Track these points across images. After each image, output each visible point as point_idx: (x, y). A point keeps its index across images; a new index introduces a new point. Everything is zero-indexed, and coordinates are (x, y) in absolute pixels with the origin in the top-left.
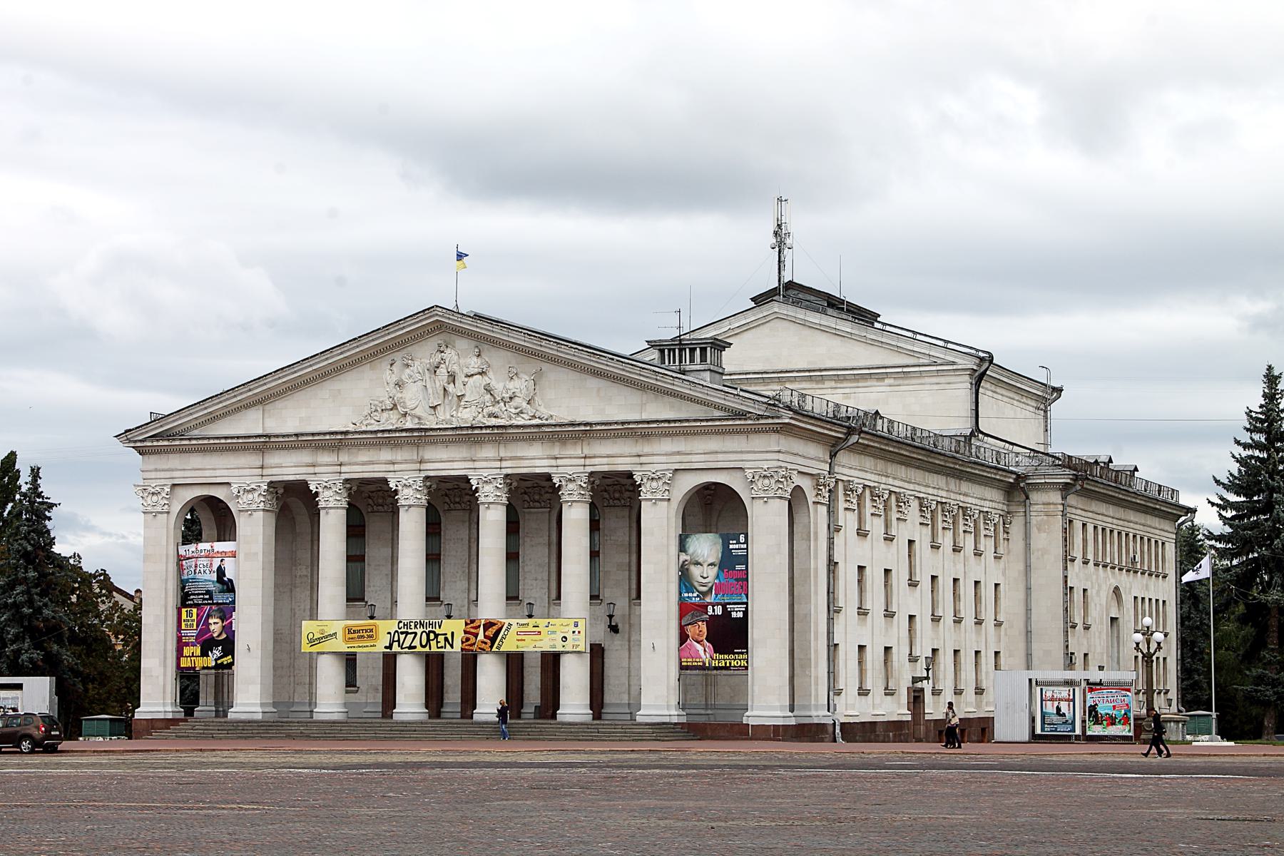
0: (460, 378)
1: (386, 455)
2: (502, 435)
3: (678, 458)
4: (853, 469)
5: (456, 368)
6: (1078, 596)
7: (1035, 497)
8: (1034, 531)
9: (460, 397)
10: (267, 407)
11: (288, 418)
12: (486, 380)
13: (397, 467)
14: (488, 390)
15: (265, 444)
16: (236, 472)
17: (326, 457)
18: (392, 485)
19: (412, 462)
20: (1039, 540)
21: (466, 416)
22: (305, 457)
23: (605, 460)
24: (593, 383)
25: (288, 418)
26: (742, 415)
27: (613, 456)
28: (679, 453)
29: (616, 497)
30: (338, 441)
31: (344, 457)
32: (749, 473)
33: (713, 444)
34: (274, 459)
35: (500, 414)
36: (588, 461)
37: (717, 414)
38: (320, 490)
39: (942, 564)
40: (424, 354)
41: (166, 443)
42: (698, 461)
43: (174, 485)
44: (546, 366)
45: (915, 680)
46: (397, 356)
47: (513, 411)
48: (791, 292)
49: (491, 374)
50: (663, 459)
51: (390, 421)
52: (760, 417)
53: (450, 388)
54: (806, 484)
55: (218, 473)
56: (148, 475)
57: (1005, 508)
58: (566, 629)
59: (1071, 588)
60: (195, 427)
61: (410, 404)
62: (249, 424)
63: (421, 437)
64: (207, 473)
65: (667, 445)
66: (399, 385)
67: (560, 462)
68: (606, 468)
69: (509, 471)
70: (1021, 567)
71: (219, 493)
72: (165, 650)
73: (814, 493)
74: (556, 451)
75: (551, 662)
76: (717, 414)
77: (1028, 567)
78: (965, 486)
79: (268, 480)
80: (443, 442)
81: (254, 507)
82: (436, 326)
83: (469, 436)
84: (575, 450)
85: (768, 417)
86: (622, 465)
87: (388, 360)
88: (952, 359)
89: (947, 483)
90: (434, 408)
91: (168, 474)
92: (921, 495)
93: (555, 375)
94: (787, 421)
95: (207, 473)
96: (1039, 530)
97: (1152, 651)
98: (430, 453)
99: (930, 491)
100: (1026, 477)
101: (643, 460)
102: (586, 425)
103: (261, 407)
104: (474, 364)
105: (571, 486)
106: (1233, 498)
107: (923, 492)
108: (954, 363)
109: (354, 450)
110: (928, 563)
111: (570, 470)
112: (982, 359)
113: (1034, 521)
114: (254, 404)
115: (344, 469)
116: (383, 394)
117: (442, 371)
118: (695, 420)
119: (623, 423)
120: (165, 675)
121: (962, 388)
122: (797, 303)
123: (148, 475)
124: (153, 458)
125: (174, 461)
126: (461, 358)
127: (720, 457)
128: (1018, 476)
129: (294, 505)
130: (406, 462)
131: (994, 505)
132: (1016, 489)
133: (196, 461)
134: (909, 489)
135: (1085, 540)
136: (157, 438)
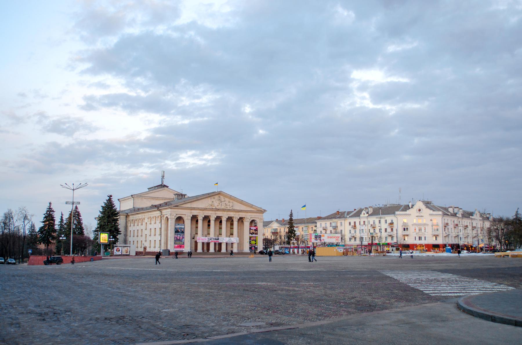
1: (210, 212)
2: (229, 210)
11: (195, 205)
15: (194, 209)
17: (201, 212)
21: (223, 207)
22: (198, 211)
27: (242, 215)
29: (241, 220)
31: (204, 212)
33: (255, 214)
34: (193, 211)
40: (216, 197)
42: (253, 216)
46: (212, 197)
58: (234, 239)
63: (218, 210)
65: (249, 214)
74: (235, 213)
75: (208, 244)
83: (224, 210)
84: (237, 214)
86: (243, 216)
93: (235, 203)
98: (216, 212)
116: (210, 203)
133: (180, 210)
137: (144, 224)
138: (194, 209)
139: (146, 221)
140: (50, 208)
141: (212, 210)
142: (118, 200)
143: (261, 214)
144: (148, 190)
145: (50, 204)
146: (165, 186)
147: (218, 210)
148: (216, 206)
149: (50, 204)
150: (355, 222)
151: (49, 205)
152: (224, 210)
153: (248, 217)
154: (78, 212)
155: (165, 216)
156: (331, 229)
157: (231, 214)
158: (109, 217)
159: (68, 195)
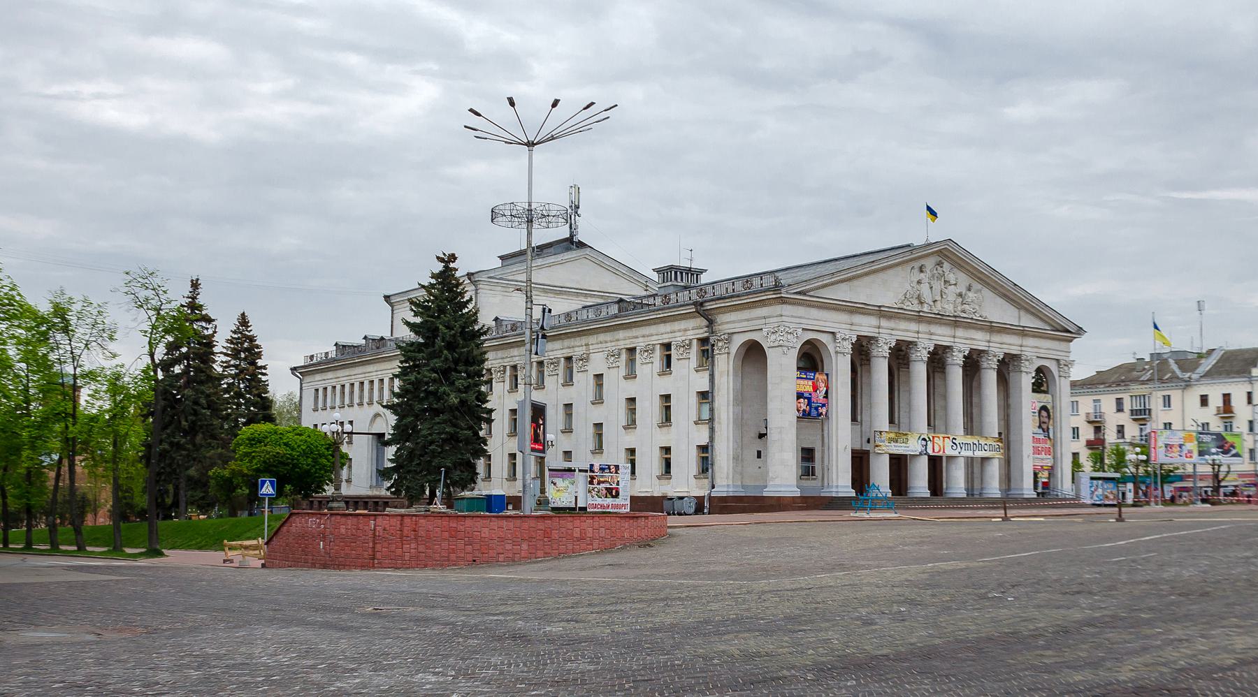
1: (913, 326)
17: (884, 323)
21: (949, 309)
22: (873, 321)
27: (1011, 344)
34: (858, 319)
42: (1043, 353)
46: (917, 264)
63: (939, 319)
71: (824, 338)
91: (798, 320)
93: (987, 293)
125: (801, 311)
129: (862, 352)
133: (814, 312)
137: (583, 381)
139: (598, 363)
140: (194, 306)
141: (919, 318)
142: (387, 298)
143: (1062, 345)
144: (499, 263)
145: (195, 285)
146: (581, 245)
147: (939, 319)
149: (195, 285)
150: (1227, 398)
151: (188, 289)
152: (956, 322)
154: (251, 339)
155: (739, 340)
156: (1125, 418)
157: (979, 340)
158: (444, 353)
159: (502, 175)
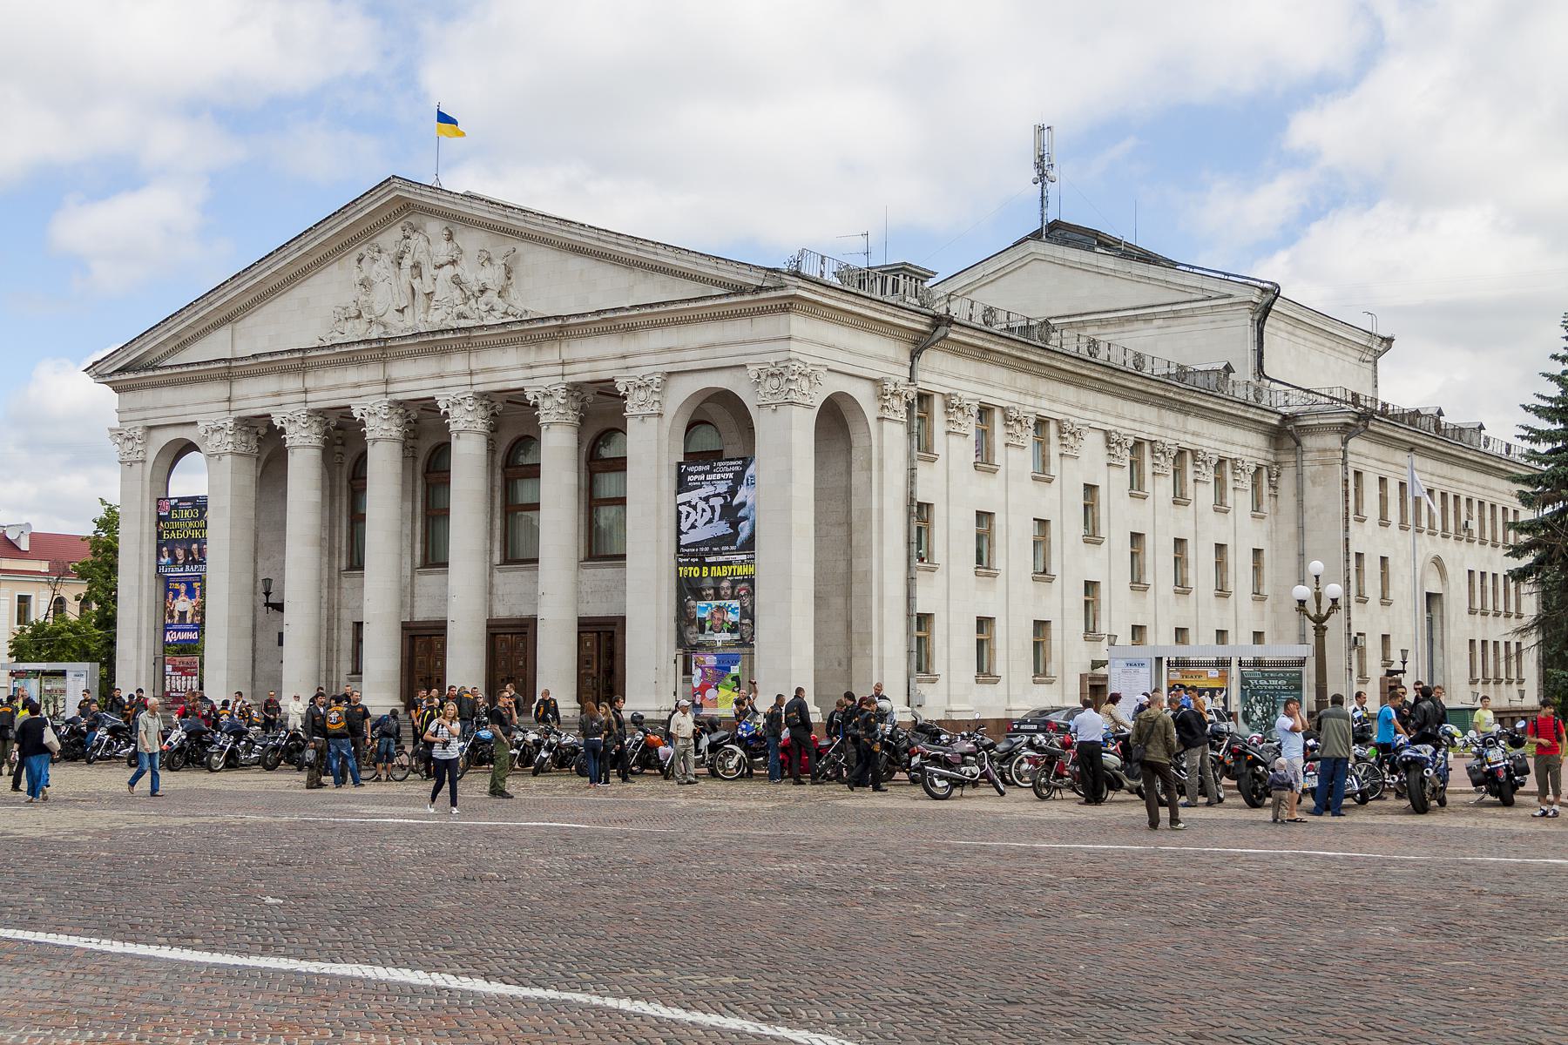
0: (428, 271)
1: (352, 375)
3: (669, 357)
4: (942, 372)
5: (423, 258)
6: (1372, 568)
7: (1309, 442)
8: (1308, 484)
9: (429, 295)
10: (239, 326)
12: (458, 270)
13: (362, 391)
14: (457, 281)
15: (228, 371)
16: (204, 408)
17: (292, 383)
18: (356, 414)
19: (377, 382)
20: (1313, 495)
21: (437, 319)
22: (270, 384)
23: (586, 366)
24: (576, 263)
25: (261, 333)
26: (740, 290)
27: (594, 359)
28: (669, 350)
29: (601, 416)
30: (299, 362)
31: (310, 381)
32: (752, 372)
35: (469, 313)
36: (568, 369)
37: (717, 291)
38: (286, 425)
39: (1159, 517)
40: (390, 238)
41: (132, 376)
42: (693, 359)
43: (151, 428)
44: (522, 247)
45: (1096, 664)
46: (363, 249)
47: (483, 308)
48: (1057, 232)
49: (463, 263)
50: (652, 359)
51: (355, 331)
52: (760, 289)
53: (416, 283)
54: (862, 393)
55: (188, 410)
56: (128, 416)
57: (1270, 457)
59: (1359, 556)
60: (167, 355)
61: (378, 309)
62: (216, 346)
63: (382, 350)
64: (178, 411)
65: (656, 339)
66: (365, 284)
67: (535, 372)
68: (588, 377)
69: (481, 388)
70: (1291, 528)
72: (139, 629)
73: (879, 405)
74: (531, 356)
76: (717, 291)
77: (1301, 529)
78: (1193, 423)
79: (235, 415)
80: (410, 355)
81: (221, 450)
82: (398, 207)
83: (433, 344)
84: (551, 354)
85: (768, 289)
86: (604, 371)
87: (355, 256)
88: (1228, 291)
89: (1159, 417)
90: (401, 311)
92: (1108, 428)
94: (792, 292)
95: (178, 411)
96: (1314, 483)
97: (1324, 612)
98: (399, 370)
99: (1126, 423)
100: (1294, 417)
101: (629, 362)
102: (556, 318)
103: (229, 326)
104: (443, 250)
105: (548, 403)
106: (1544, 425)
107: (1099, 420)
108: (1230, 296)
109: (320, 373)
110: (1119, 513)
111: (546, 382)
112: (1264, 290)
113: (1308, 471)
114: (217, 326)
115: (310, 397)
117: (407, 262)
118: (681, 301)
119: (598, 312)
120: (139, 658)
121: (1243, 324)
122: (1066, 243)
123: (128, 416)
124: (129, 395)
125: (146, 397)
126: (431, 242)
127: (719, 351)
128: (1285, 417)
129: (265, 445)
130: (371, 383)
131: (1250, 452)
132: (1286, 434)
133: (167, 395)
134: (1076, 417)
135: (1383, 499)
136: (130, 371)
138: (228, 371)
147: (382, 350)
148: (391, 318)
152: (433, 344)
153: (660, 378)
